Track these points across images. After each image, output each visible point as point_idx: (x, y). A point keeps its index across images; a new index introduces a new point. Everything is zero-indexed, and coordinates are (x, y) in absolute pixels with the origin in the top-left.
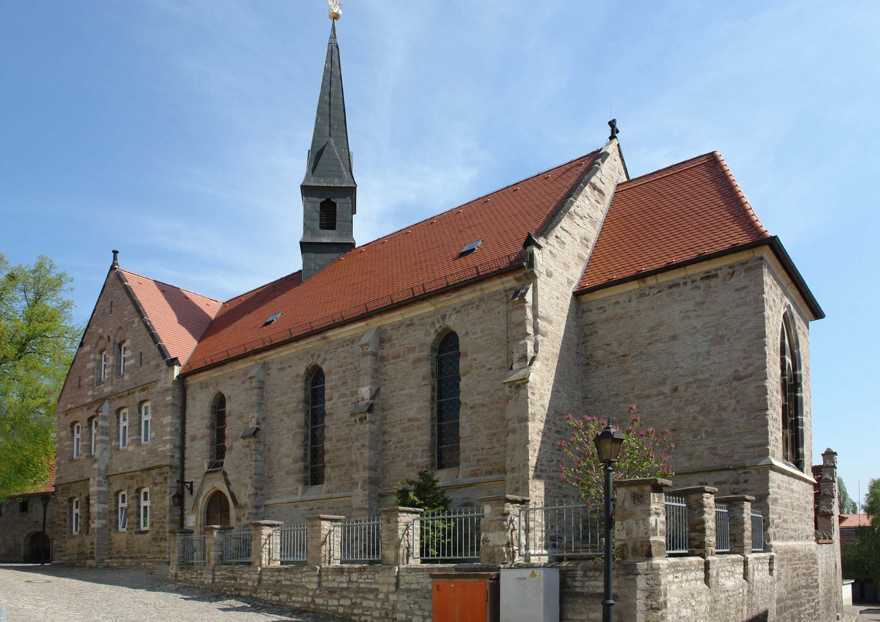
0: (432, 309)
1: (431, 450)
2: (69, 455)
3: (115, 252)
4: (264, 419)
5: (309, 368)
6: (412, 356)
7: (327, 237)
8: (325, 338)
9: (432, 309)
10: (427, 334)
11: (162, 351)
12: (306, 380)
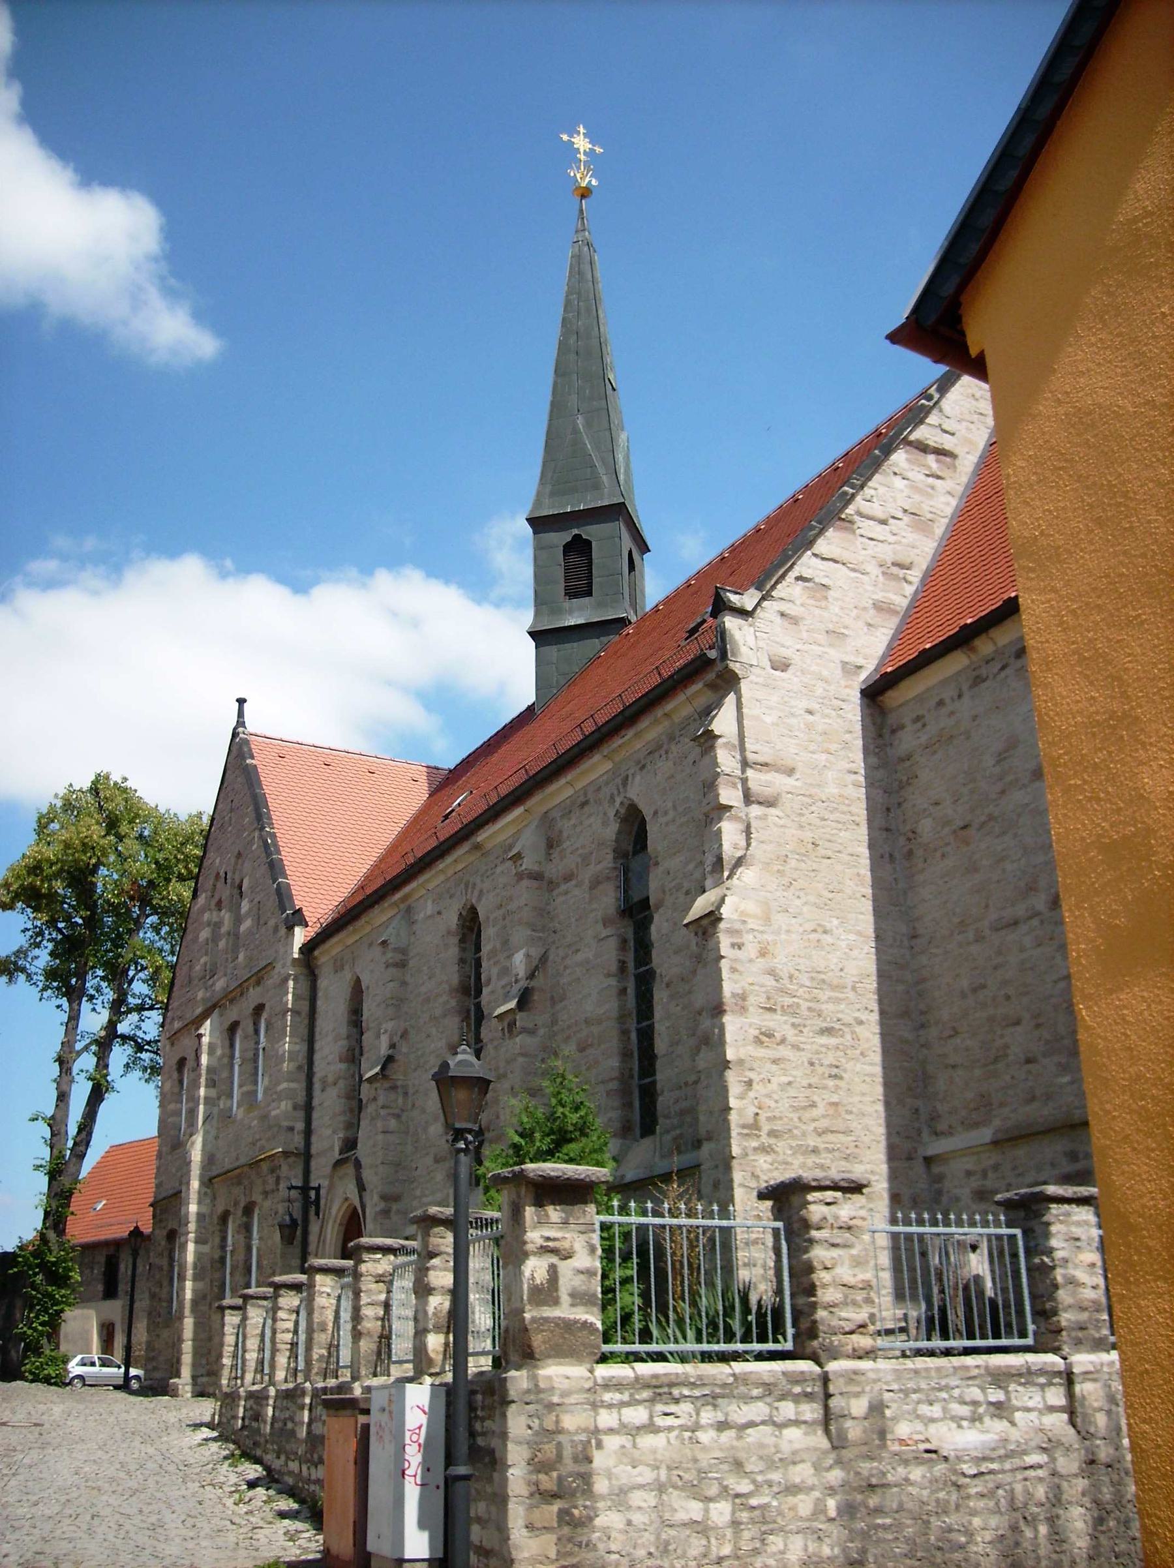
0: (608, 765)
1: (624, 1092)
2: (172, 1132)
3: (241, 701)
4: (404, 1035)
5: (464, 913)
6: (587, 875)
7: (577, 615)
8: (477, 847)
9: (608, 765)
10: (605, 824)
11: (283, 896)
12: (462, 941)
